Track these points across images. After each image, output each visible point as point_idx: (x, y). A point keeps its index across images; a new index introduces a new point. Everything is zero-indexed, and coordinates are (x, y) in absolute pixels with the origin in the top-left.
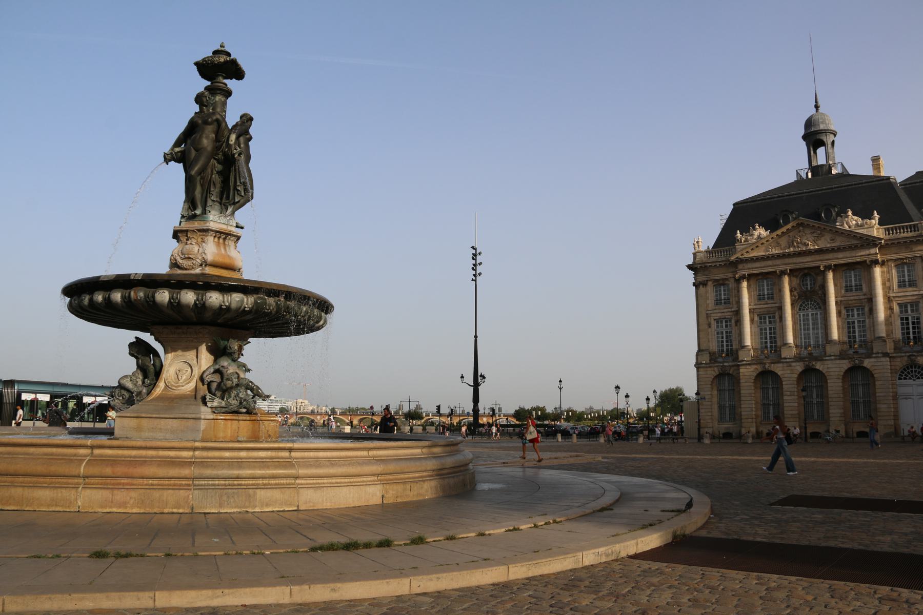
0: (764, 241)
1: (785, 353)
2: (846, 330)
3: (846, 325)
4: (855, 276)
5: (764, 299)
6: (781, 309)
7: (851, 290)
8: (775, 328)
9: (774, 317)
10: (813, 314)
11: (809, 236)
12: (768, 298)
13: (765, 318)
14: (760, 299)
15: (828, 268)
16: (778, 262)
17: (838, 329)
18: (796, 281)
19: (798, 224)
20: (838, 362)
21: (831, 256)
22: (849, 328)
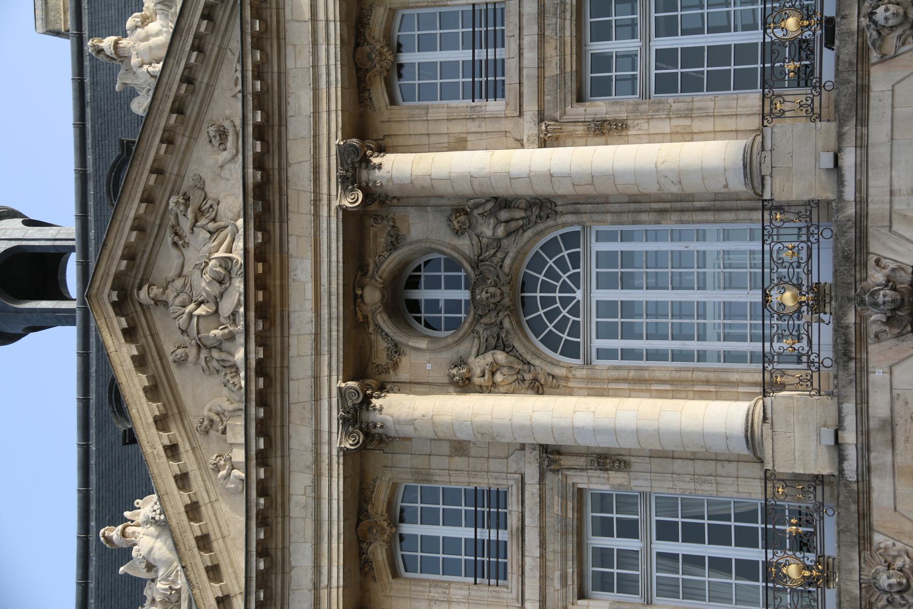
0: (178, 500)
1: (801, 448)
2: (704, 99)
3: (675, 100)
4: (426, 44)
5: (500, 548)
6: (551, 455)
7: (498, 66)
8: (666, 504)
9: (603, 502)
10: (605, 282)
11: (193, 256)
12: (500, 522)
13: (604, 556)
14: (499, 573)
15: (354, 167)
16: (300, 437)
17: (689, 135)
18: (421, 355)
19: (119, 307)
20: (878, 131)
21: (299, 153)
22: (692, 84)
